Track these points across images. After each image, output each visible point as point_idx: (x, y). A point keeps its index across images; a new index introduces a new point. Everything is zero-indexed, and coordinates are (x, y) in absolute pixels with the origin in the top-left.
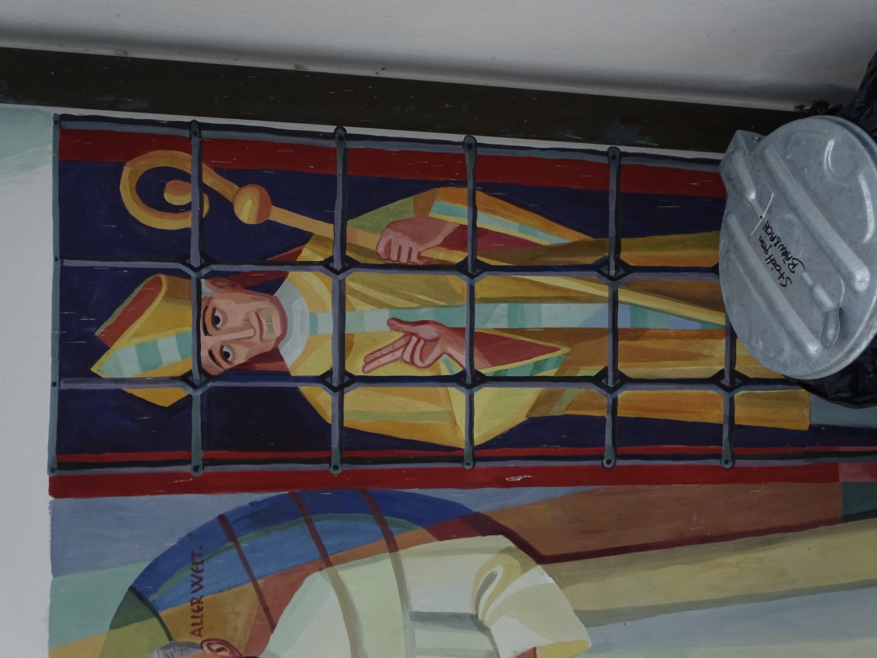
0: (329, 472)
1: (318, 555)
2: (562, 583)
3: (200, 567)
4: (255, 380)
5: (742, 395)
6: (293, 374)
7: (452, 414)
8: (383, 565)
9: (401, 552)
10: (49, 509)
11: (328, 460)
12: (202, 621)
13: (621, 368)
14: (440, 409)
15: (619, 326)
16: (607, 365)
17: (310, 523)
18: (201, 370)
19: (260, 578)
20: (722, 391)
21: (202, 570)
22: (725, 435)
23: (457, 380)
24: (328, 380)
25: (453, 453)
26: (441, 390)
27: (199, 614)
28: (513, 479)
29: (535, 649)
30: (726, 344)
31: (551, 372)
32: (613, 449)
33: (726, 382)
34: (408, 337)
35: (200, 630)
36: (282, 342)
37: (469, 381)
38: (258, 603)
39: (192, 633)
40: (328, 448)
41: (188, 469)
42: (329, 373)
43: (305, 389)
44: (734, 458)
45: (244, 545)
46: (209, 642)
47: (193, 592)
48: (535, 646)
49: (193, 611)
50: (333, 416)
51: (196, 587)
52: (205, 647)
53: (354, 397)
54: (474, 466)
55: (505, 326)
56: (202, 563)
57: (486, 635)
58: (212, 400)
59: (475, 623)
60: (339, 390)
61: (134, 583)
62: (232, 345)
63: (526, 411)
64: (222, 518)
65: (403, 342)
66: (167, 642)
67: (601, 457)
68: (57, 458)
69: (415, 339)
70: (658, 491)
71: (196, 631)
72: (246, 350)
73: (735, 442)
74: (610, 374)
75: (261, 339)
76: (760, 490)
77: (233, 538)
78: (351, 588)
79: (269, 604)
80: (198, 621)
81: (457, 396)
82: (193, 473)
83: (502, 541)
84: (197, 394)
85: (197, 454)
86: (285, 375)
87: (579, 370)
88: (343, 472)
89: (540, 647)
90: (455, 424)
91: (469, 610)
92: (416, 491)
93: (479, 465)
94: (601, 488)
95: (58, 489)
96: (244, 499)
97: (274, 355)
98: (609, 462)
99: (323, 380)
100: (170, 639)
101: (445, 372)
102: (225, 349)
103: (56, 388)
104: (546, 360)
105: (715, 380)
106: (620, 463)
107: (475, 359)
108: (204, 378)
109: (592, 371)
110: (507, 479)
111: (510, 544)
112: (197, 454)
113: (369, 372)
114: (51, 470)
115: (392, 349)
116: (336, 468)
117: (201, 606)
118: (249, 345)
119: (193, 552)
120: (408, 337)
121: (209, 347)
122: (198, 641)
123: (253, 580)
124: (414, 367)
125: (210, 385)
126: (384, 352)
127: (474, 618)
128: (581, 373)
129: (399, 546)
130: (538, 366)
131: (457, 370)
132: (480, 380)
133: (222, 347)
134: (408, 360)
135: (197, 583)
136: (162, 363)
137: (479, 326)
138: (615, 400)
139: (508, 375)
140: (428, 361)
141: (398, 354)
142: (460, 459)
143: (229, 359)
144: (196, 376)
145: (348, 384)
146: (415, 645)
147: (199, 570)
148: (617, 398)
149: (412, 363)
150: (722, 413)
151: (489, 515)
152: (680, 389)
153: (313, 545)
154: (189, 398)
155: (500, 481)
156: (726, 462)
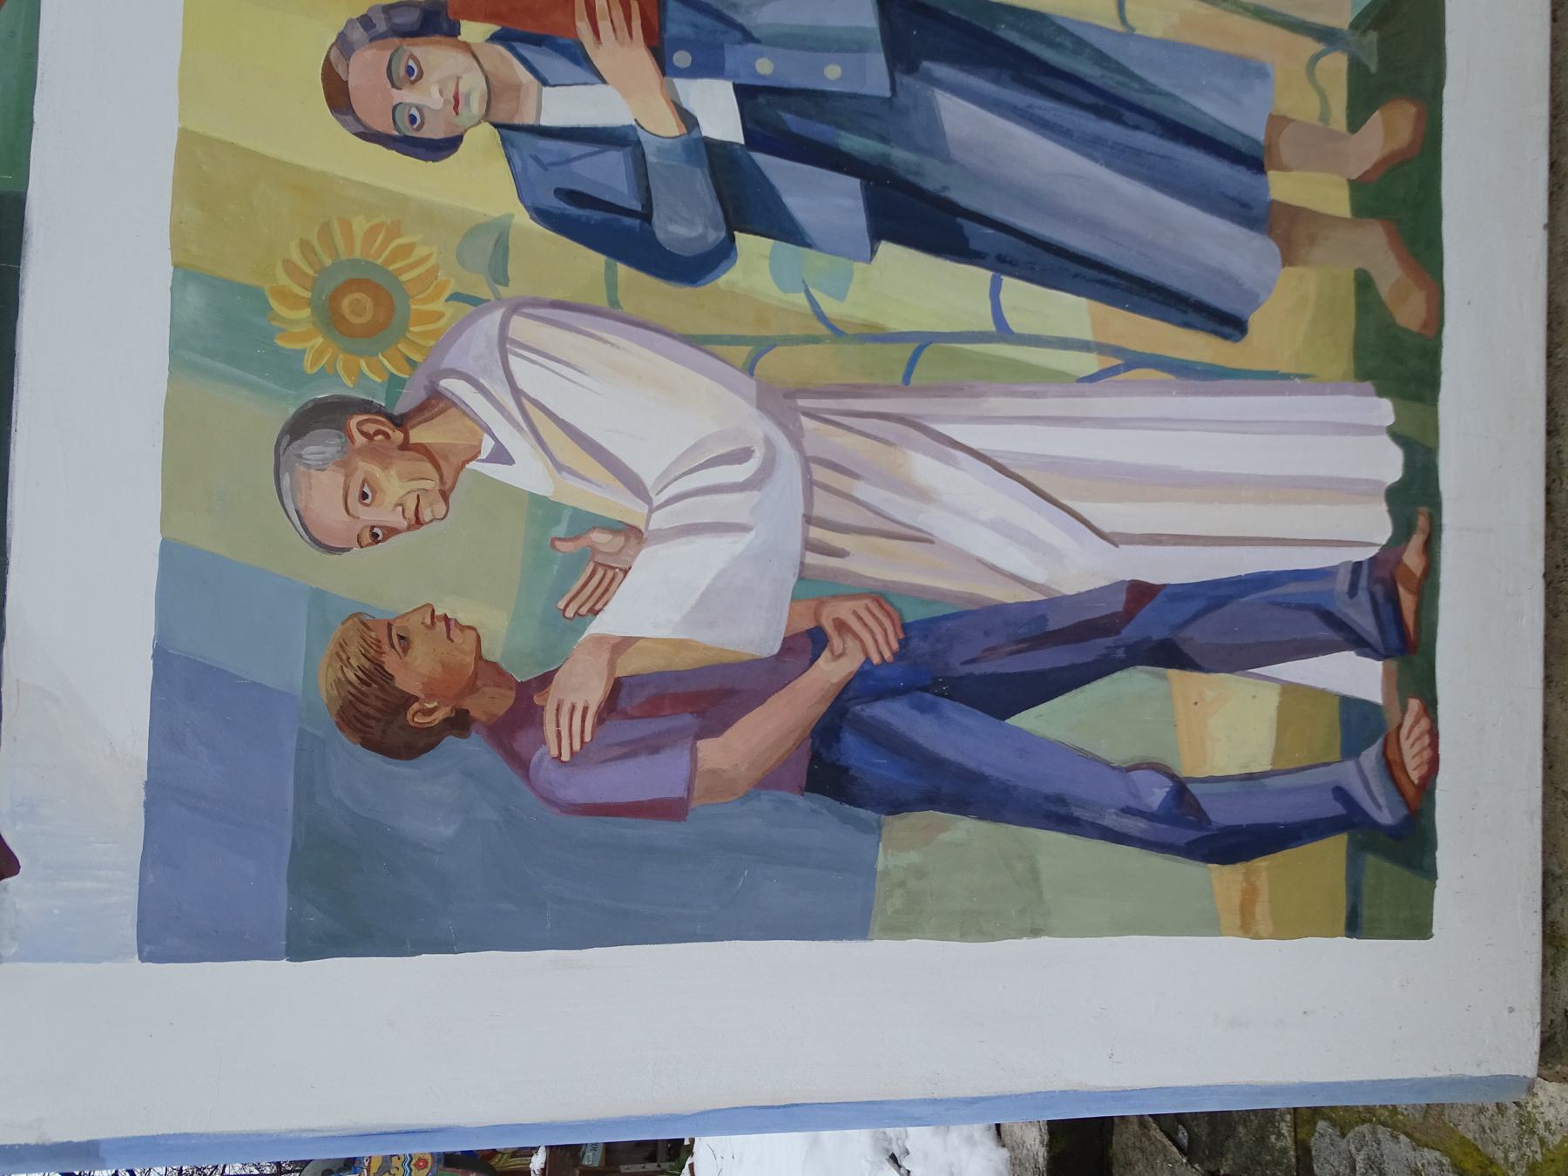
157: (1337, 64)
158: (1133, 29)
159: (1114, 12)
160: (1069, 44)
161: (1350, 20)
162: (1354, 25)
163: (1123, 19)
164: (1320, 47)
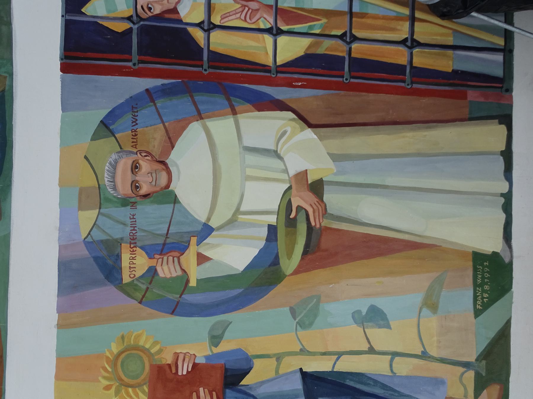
0: (202, 72)
1: (196, 113)
2: (321, 138)
3: (136, 114)
4: (164, 22)
5: (417, 51)
6: (184, 21)
7: (265, 48)
8: (229, 121)
9: (238, 115)
10: (60, 78)
11: (202, 66)
12: (137, 141)
13: (354, 32)
14: (259, 45)
15: (353, 11)
16: (346, 30)
17: (192, 97)
18: (137, 15)
19: (166, 122)
20: (406, 49)
21: (137, 116)
22: (408, 71)
23: (269, 31)
24: (202, 25)
25: (266, 68)
26: (260, 35)
27: (135, 137)
28: (297, 84)
29: (306, 170)
30: (409, 24)
31: (317, 31)
32: (348, 73)
33: (409, 43)
34: (244, 7)
35: (136, 145)
36: (178, 5)
37: (274, 32)
38: (165, 134)
39: (132, 146)
40: (201, 59)
41: (130, 64)
42: (203, 22)
43: (190, 29)
44: (412, 83)
45: (158, 105)
46: (141, 152)
47: (133, 126)
48: (307, 169)
49: (132, 135)
50: (204, 44)
51: (134, 124)
52: (138, 154)
53: (216, 36)
54: (277, 75)
55: (294, 6)
56: (137, 112)
57: (281, 161)
58: (143, 30)
59: (276, 154)
60: (208, 31)
61: (103, 119)
62: (153, 4)
63: (304, 50)
64: (147, 90)
65: (241, 10)
66: (119, 150)
67: (343, 77)
68: (64, 53)
69: (247, 9)
70: (372, 96)
71: (134, 145)
72: (160, 7)
73: (412, 75)
74: (348, 34)
75: (168, 2)
76: (425, 101)
77: (153, 101)
78: (213, 131)
79: (171, 135)
80: (135, 140)
81: (268, 39)
82: (133, 67)
83: (290, 115)
84: (135, 27)
85: (135, 57)
86: (180, 21)
87: (332, 31)
88: (209, 73)
89: (309, 169)
90: (267, 53)
91: (273, 148)
92: (246, 85)
93: (279, 75)
94: (342, 92)
95: (65, 69)
96: (159, 82)
97: (175, 11)
98: (346, 79)
99: (200, 25)
100: (121, 148)
101: (262, 26)
102: (150, 6)
103: (64, 18)
104: (315, 25)
105: (403, 42)
106: (352, 80)
107: (278, 22)
108: (139, 19)
109: (339, 33)
110: (293, 84)
111: (295, 116)
112: (135, 57)
113: (223, 23)
114: (61, 59)
115: (235, 13)
116: (206, 70)
117: (136, 133)
118: (162, 5)
119: (132, 106)
120: (244, 7)
121: (141, 4)
122: (135, 150)
123: (163, 122)
124: (246, 23)
125: (142, 23)
126: (231, 14)
127: (276, 152)
128: (334, 33)
129: (237, 112)
130: (310, 27)
131: (269, 26)
132: (280, 32)
133: (148, 5)
134: (243, 19)
135: (135, 122)
136: (117, 10)
137: (280, 5)
138: (350, 49)
139: (295, 31)
140: (254, 20)
141: (238, 15)
142: (269, 71)
143: (152, 11)
144: (135, 18)
145: (213, 29)
146: (245, 163)
147: (136, 115)
148: (351, 47)
149: (245, 20)
150: (406, 59)
151: (284, 101)
152: (385, 45)
153: (193, 108)
154: (131, 29)
155: (290, 84)
156: (408, 85)
157: (470, 375)
158: (395, 374)
159: (388, 368)
160: (372, 383)
161: (475, 358)
162: (477, 360)
163: (392, 371)
164: (465, 369)
